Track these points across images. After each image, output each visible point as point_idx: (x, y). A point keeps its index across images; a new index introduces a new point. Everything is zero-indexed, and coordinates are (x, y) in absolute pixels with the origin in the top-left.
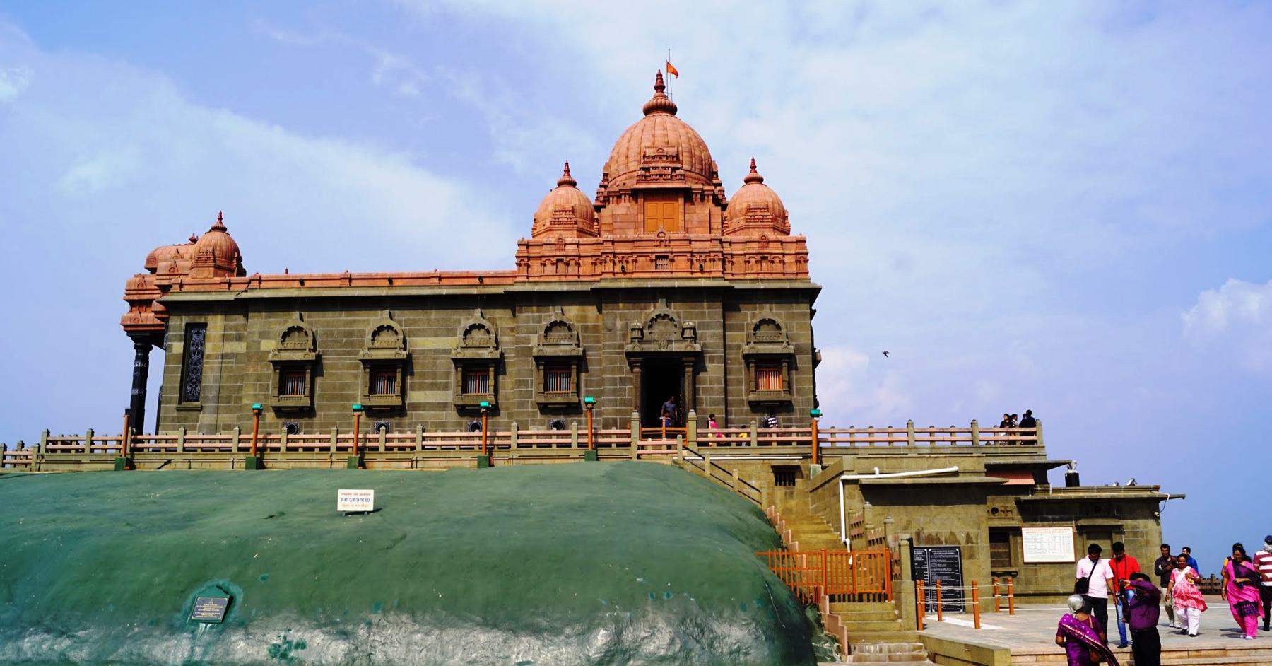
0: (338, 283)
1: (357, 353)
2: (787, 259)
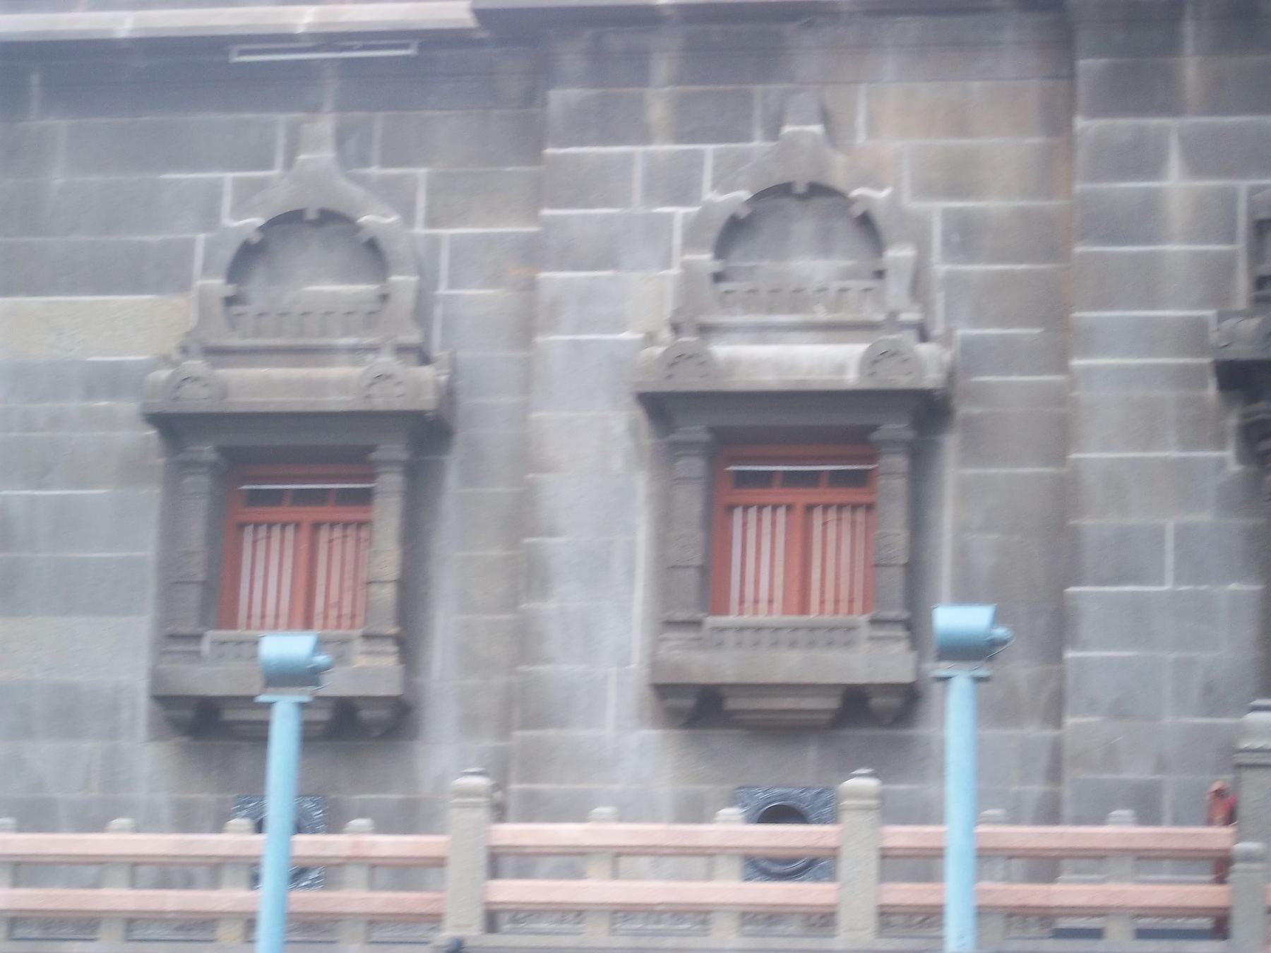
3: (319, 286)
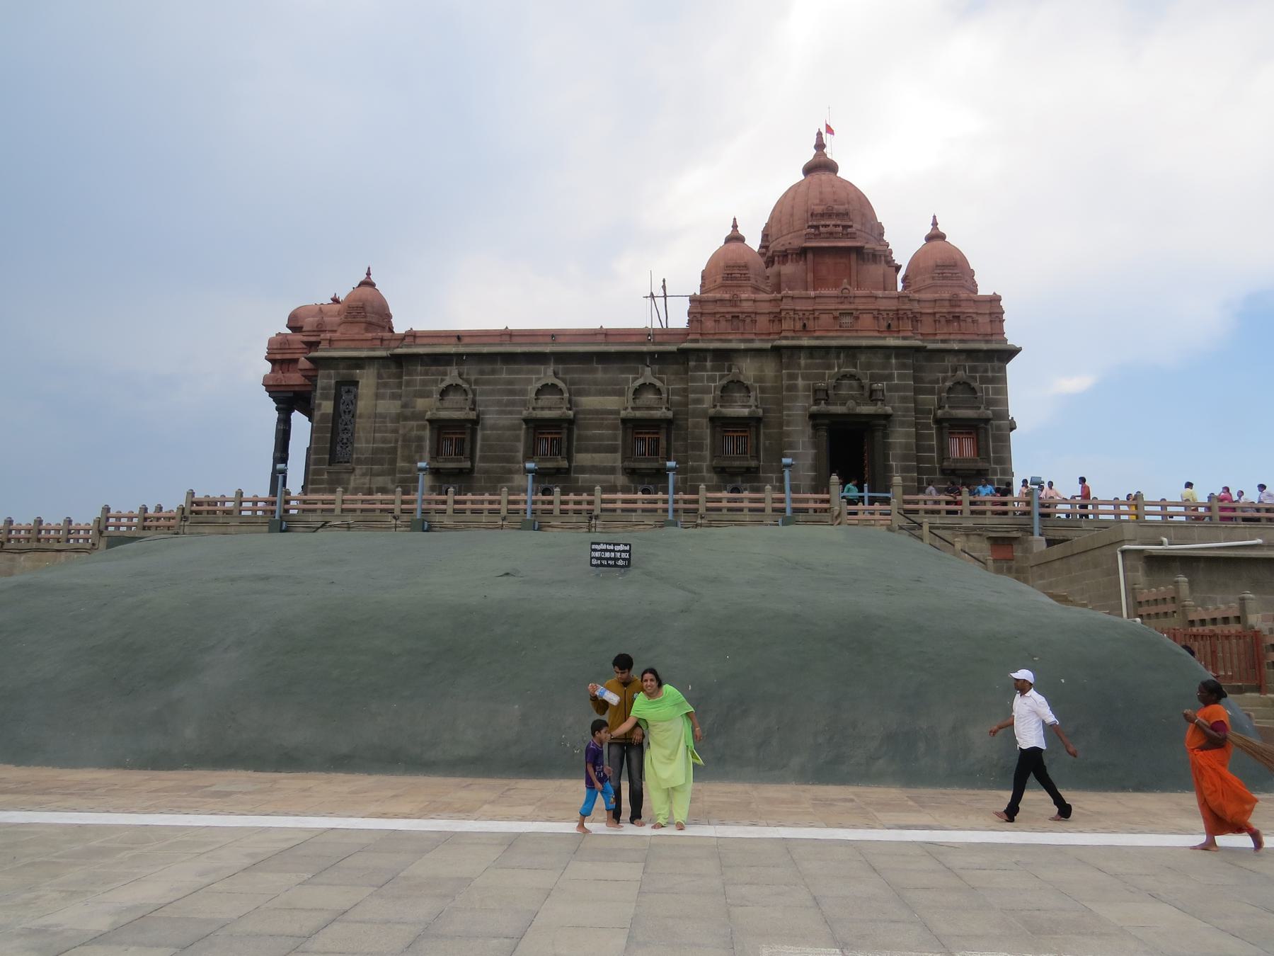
0: (497, 340)
1: (520, 413)
2: (980, 319)
3: (649, 397)
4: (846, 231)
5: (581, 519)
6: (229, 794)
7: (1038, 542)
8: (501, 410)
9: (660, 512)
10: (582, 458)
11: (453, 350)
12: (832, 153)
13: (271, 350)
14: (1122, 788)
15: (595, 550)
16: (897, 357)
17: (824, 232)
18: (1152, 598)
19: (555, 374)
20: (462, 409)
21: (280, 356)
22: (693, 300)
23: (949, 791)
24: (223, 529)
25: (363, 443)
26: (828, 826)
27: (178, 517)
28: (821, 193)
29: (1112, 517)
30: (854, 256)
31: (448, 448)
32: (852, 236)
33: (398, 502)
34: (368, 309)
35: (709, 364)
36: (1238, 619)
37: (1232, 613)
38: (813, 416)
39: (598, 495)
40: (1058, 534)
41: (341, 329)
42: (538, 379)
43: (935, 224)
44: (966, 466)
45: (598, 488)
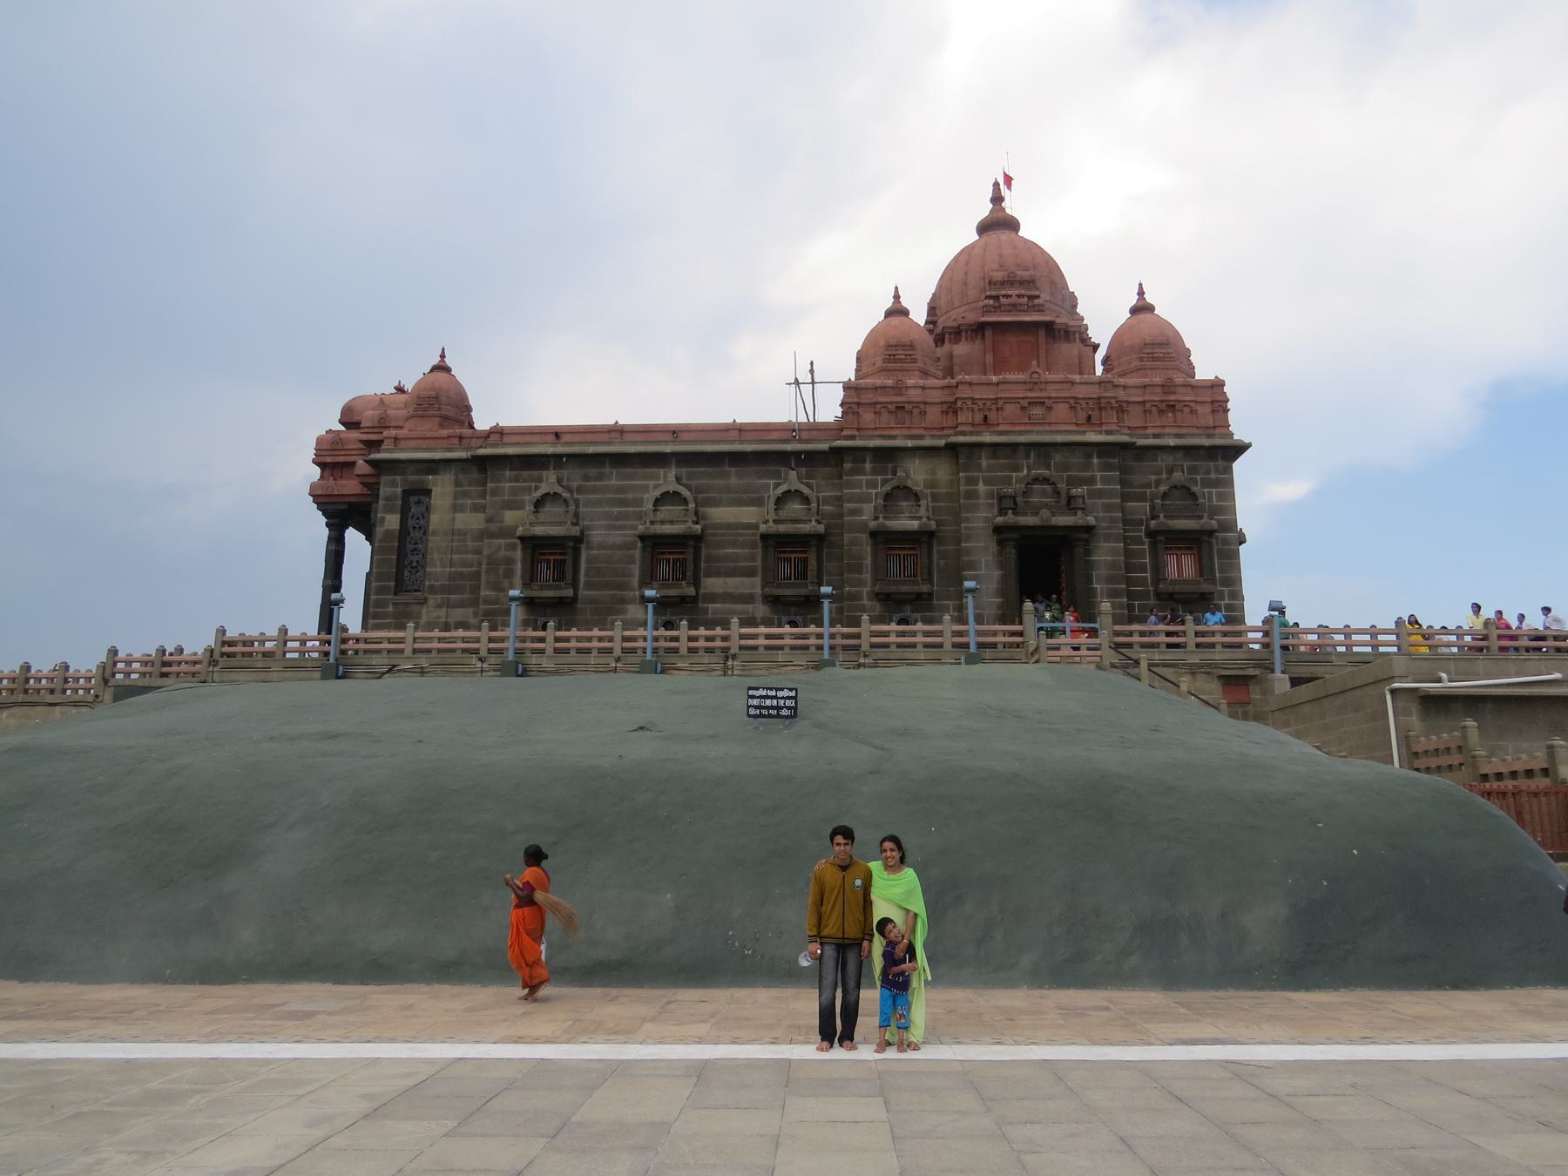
0: (605, 437)
2: (1200, 409)
3: (796, 507)
4: (1032, 303)
5: (714, 660)
6: (309, 1015)
7: (1280, 682)
8: (611, 525)
9: (813, 649)
10: (712, 584)
11: (550, 450)
12: (1012, 207)
13: (319, 451)
14: (1437, 984)
15: (753, 697)
16: (1099, 456)
17: (1004, 306)
18: (1432, 748)
19: (678, 479)
20: (561, 523)
21: (331, 458)
22: (848, 387)
23: (1221, 993)
24: (263, 676)
25: (437, 568)
26: (1094, 1043)
27: (206, 662)
28: (1001, 256)
29: (1369, 649)
30: (1042, 333)
31: (544, 571)
32: (1040, 309)
33: (484, 640)
34: (443, 399)
35: (868, 466)
36: (1545, 772)
37: (1537, 765)
38: (998, 530)
39: (736, 629)
40: (1304, 671)
41: (409, 425)
42: (657, 486)
43: (1141, 293)
44: (1186, 588)
45: (735, 620)
